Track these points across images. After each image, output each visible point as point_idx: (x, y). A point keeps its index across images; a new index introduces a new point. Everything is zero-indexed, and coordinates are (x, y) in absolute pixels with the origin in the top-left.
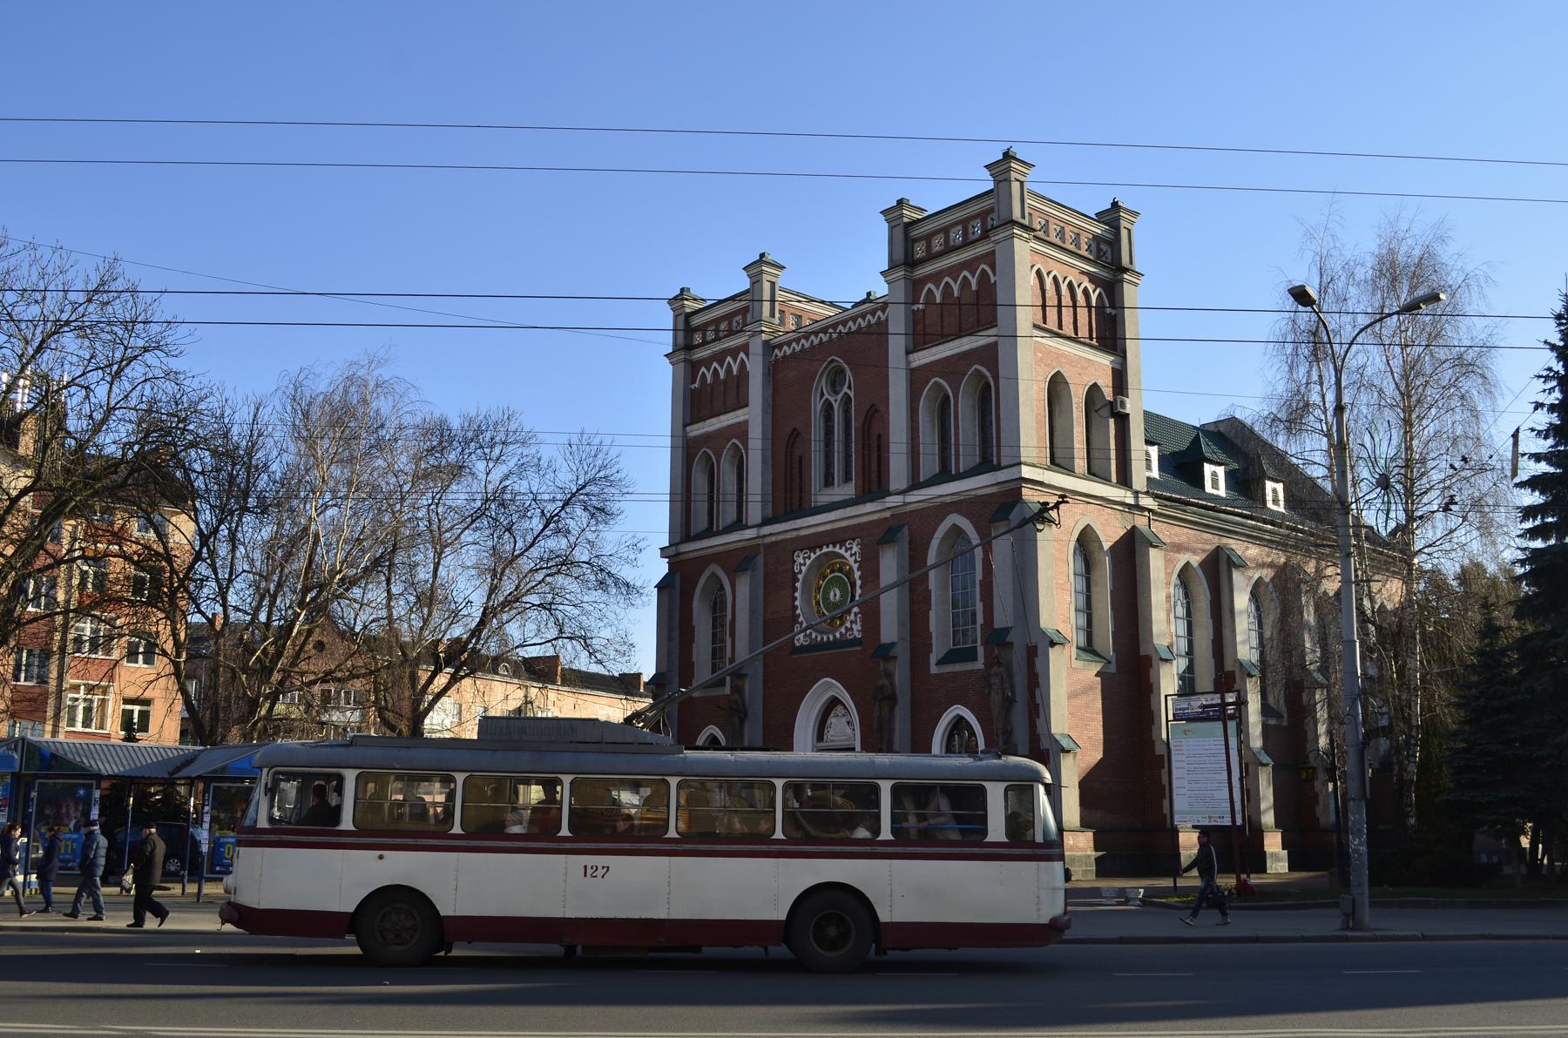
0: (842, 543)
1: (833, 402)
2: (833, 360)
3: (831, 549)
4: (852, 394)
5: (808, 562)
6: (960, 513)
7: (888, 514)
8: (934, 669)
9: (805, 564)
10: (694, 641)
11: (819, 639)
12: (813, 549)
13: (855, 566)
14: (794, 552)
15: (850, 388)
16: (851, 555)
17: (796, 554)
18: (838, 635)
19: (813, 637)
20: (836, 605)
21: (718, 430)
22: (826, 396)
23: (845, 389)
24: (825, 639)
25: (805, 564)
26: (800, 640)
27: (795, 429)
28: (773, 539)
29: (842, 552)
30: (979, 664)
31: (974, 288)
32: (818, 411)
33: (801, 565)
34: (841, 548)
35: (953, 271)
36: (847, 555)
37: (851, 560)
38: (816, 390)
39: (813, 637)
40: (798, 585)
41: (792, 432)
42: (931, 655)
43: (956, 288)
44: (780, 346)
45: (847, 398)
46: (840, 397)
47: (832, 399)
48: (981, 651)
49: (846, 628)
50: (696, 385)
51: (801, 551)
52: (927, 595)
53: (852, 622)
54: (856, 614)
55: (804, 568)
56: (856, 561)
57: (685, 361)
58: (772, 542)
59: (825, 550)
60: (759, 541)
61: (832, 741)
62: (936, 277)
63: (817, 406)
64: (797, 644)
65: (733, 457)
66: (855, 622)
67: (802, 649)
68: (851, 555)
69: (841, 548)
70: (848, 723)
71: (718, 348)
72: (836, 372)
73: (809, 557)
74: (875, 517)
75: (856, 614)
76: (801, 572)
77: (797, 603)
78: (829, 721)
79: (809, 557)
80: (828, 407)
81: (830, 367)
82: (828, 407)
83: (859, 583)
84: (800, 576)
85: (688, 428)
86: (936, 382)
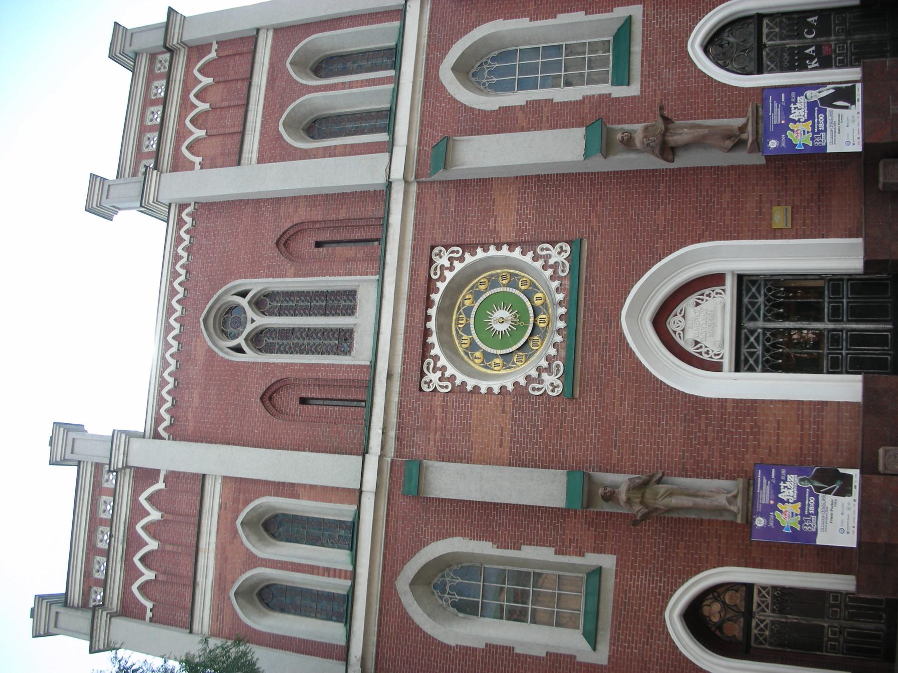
0: (430, 287)
1: (254, 325)
2: (205, 321)
3: (433, 312)
4: (257, 285)
5: (443, 361)
6: (440, 60)
7: (414, 188)
8: (633, 90)
9: (444, 369)
10: (511, 649)
11: (558, 339)
12: (426, 347)
13: (469, 259)
14: (421, 389)
15: (243, 294)
16: (451, 268)
17: (425, 387)
18: (560, 297)
19: (552, 352)
20: (520, 315)
21: (216, 559)
22: (240, 341)
23: (244, 302)
24: (561, 324)
25: (444, 369)
26: (552, 384)
27: (262, 399)
28: (392, 434)
29: (442, 286)
30: (636, 11)
31: (210, 80)
32: (256, 355)
33: (440, 380)
34: (437, 290)
35: (186, 105)
36: (449, 275)
37: (458, 266)
38: (227, 353)
39: (552, 352)
40: (471, 383)
41: (263, 402)
42: (614, 95)
43: (203, 106)
44: (158, 420)
45: (261, 303)
46: (250, 313)
47: (249, 327)
48: (621, 12)
49: (552, 278)
50: (149, 605)
51: (423, 375)
52: (534, 106)
53: (545, 267)
54: (535, 258)
55: (451, 371)
56: (461, 259)
57: (112, 615)
58: (398, 439)
59: (432, 325)
60: (389, 460)
61: (722, 345)
62: (181, 134)
63: (251, 356)
64: (559, 390)
65: (261, 539)
66: (549, 257)
67: (569, 377)
68: (451, 268)
69: (437, 290)
70: (697, 304)
71: (120, 547)
72: (223, 331)
73: (436, 358)
74: (411, 213)
75: (535, 258)
76: (452, 378)
77: (496, 387)
78: (691, 349)
79: (436, 358)
80: (258, 340)
81: (212, 331)
82: (258, 340)
83: (493, 251)
84: (460, 378)
85: (196, 627)
86: (284, 124)
